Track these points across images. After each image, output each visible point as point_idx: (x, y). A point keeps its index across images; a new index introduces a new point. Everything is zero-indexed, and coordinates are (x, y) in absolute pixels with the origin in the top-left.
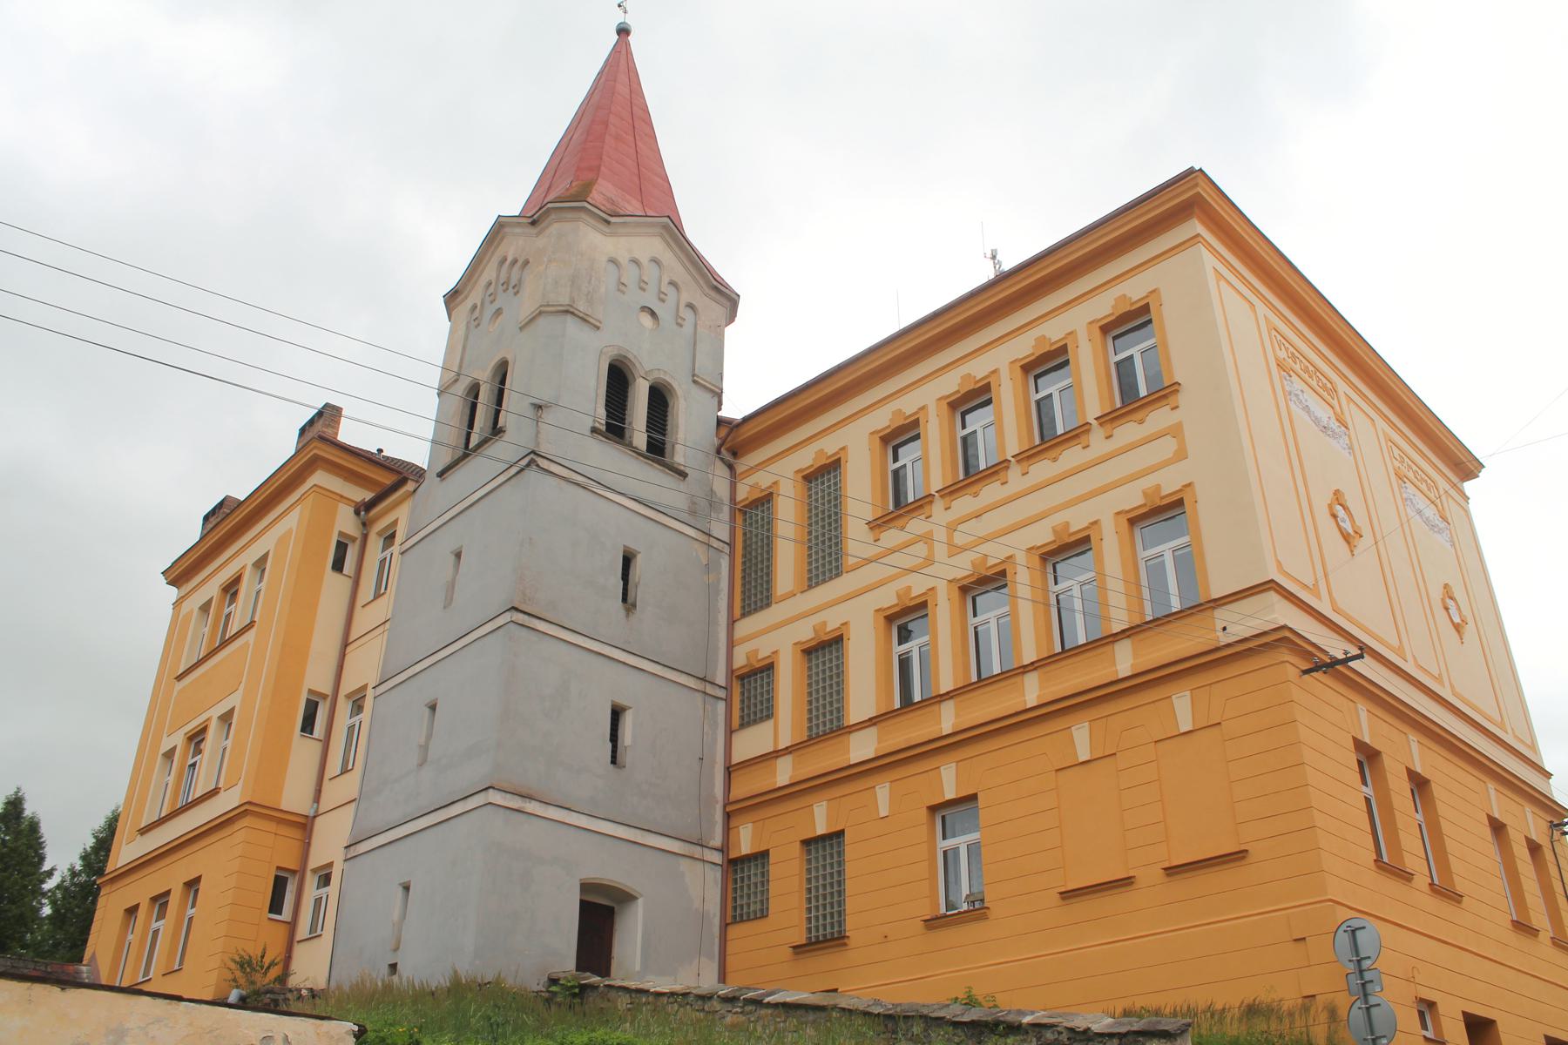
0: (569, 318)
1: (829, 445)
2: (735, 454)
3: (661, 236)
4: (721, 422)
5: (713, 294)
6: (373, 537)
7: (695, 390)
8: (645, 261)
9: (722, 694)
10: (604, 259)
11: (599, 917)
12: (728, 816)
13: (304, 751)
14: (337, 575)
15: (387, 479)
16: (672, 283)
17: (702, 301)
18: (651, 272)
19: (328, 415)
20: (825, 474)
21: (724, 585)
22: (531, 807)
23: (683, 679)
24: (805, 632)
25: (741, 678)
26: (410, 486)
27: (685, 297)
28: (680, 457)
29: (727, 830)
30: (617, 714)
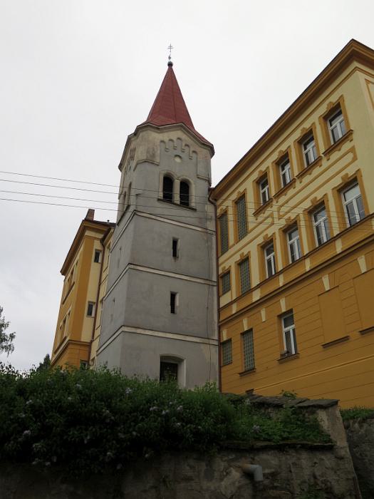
0: (147, 164)
1: (241, 189)
2: (216, 200)
3: (180, 130)
4: (211, 190)
5: (203, 146)
6: (106, 249)
7: (199, 181)
8: (175, 140)
9: (215, 284)
10: (159, 141)
11: (170, 367)
12: (219, 327)
13: (88, 322)
14: (96, 264)
15: (106, 228)
16: (186, 145)
17: (199, 149)
18: (176, 143)
19: (91, 212)
20: (242, 199)
21: (214, 246)
22: (139, 331)
23: (198, 280)
24: (237, 258)
25: (222, 277)
26: (112, 230)
27: (192, 149)
28: (193, 205)
29: (220, 333)
30: (173, 296)
